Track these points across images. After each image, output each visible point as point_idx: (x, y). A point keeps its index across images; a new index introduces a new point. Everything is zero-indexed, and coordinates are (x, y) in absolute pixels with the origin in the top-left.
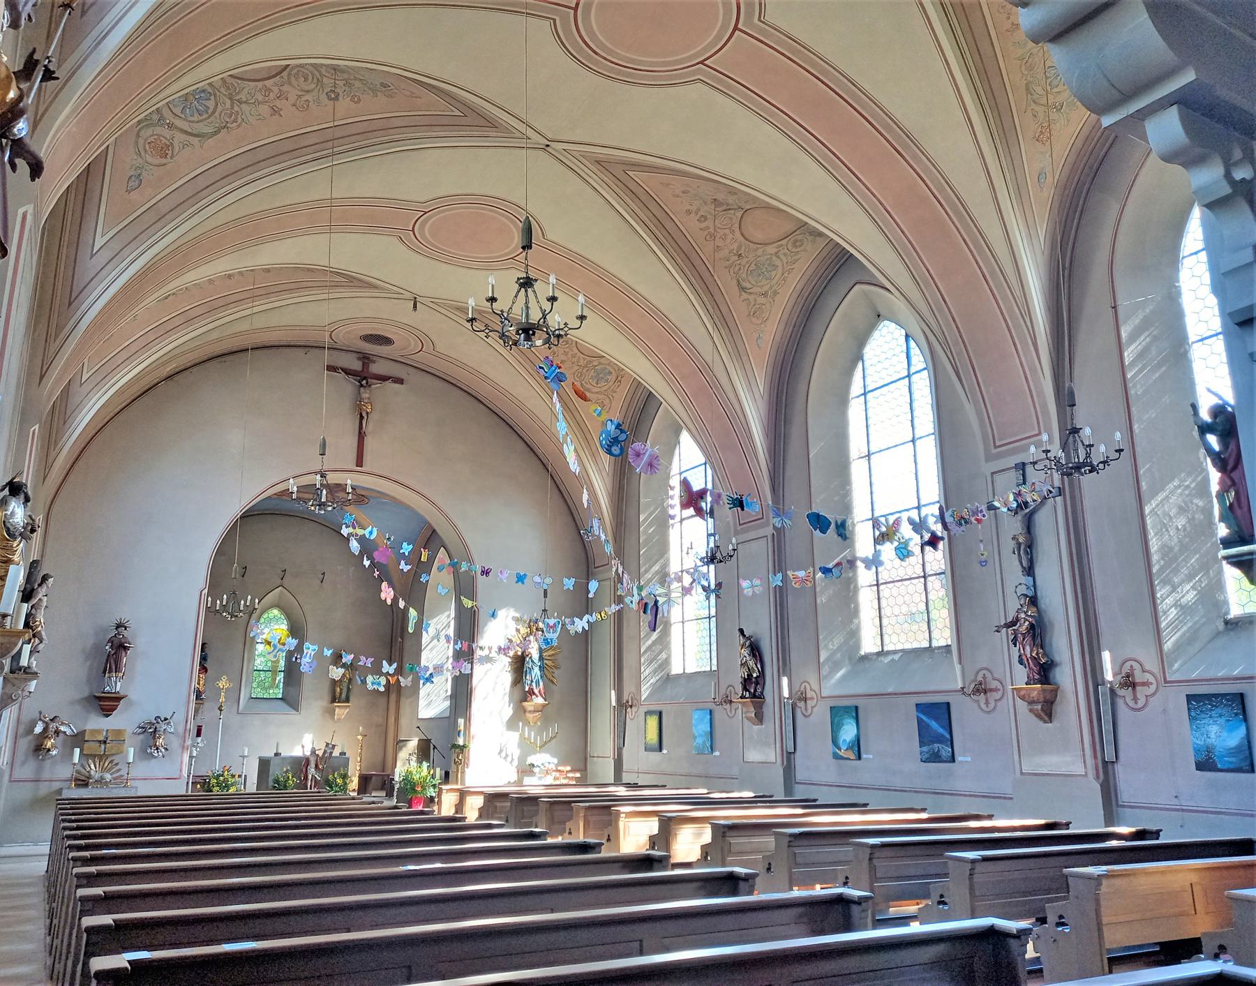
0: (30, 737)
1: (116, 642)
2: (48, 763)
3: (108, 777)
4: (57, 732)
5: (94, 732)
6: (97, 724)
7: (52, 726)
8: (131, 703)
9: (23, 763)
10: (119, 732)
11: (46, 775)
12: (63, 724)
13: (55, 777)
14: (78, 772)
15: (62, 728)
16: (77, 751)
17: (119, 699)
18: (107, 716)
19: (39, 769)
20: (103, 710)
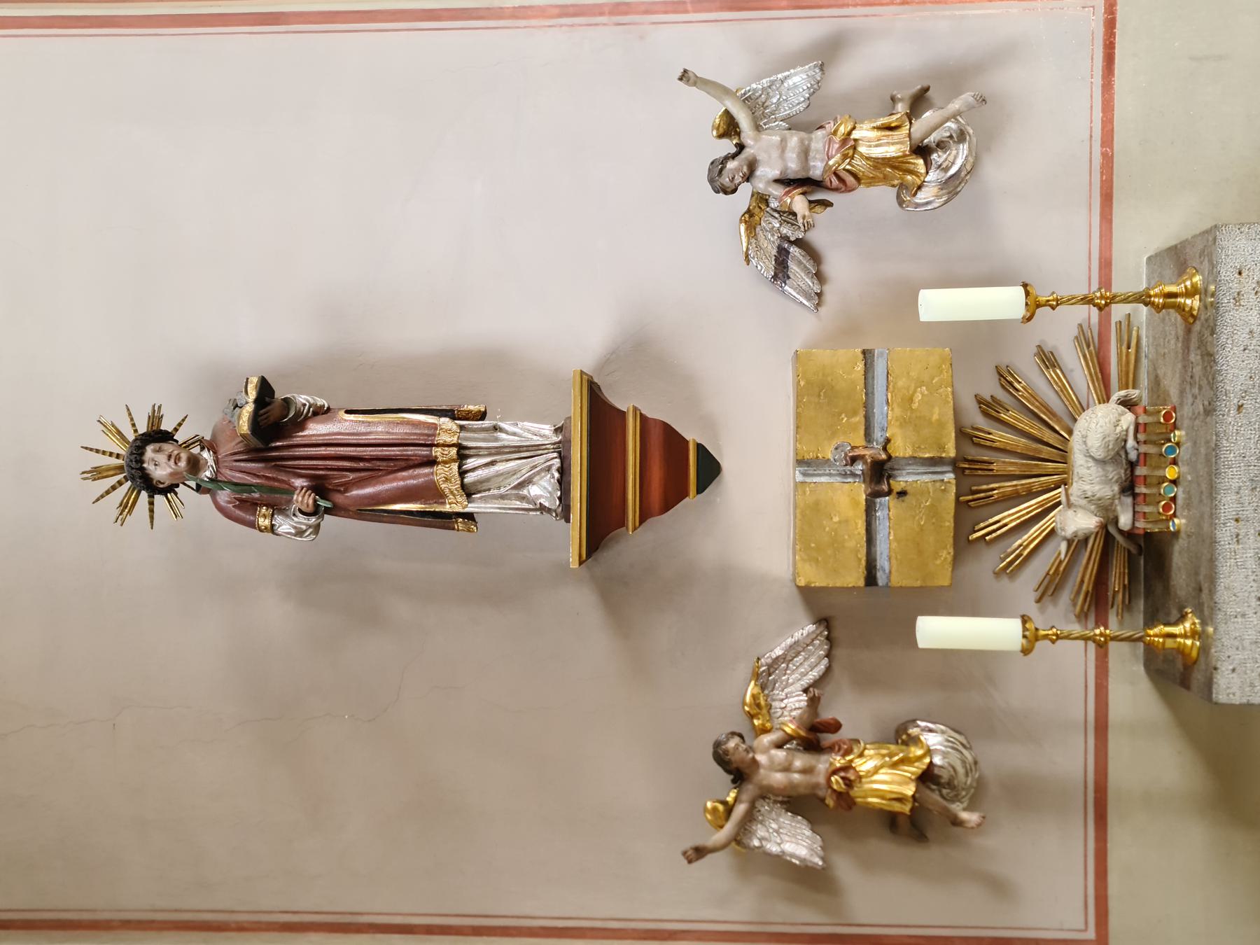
0: (846, 870)
1: (249, 473)
2: (1001, 758)
3: (1100, 426)
4: (815, 735)
5: (809, 522)
6: (763, 516)
7: (775, 764)
8: (639, 350)
9: (998, 887)
10: (815, 394)
11: (1069, 759)
12: (760, 708)
13: (1079, 706)
14: (1050, 589)
15: (790, 704)
16: (936, 630)
17: (602, 416)
18: (710, 469)
19: (1025, 795)
20: (674, 494)
